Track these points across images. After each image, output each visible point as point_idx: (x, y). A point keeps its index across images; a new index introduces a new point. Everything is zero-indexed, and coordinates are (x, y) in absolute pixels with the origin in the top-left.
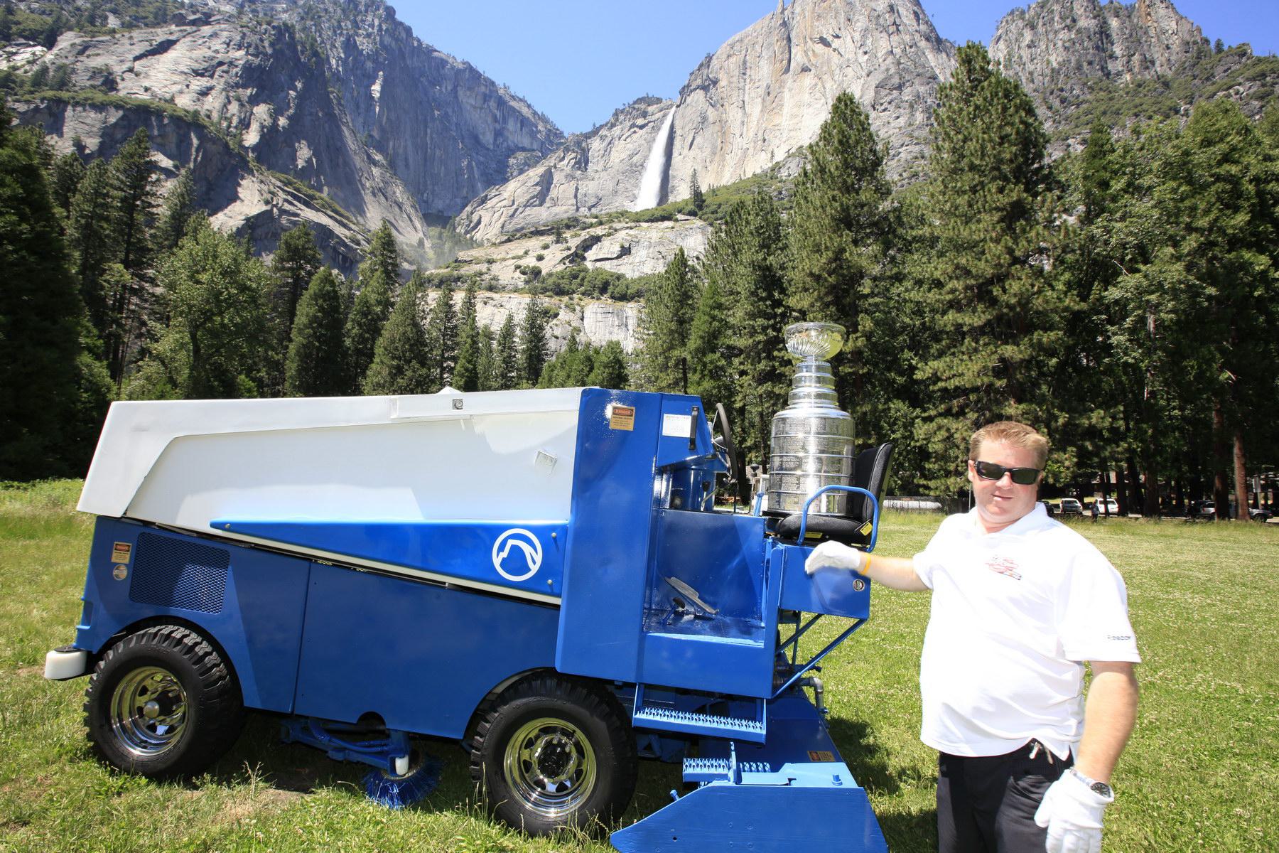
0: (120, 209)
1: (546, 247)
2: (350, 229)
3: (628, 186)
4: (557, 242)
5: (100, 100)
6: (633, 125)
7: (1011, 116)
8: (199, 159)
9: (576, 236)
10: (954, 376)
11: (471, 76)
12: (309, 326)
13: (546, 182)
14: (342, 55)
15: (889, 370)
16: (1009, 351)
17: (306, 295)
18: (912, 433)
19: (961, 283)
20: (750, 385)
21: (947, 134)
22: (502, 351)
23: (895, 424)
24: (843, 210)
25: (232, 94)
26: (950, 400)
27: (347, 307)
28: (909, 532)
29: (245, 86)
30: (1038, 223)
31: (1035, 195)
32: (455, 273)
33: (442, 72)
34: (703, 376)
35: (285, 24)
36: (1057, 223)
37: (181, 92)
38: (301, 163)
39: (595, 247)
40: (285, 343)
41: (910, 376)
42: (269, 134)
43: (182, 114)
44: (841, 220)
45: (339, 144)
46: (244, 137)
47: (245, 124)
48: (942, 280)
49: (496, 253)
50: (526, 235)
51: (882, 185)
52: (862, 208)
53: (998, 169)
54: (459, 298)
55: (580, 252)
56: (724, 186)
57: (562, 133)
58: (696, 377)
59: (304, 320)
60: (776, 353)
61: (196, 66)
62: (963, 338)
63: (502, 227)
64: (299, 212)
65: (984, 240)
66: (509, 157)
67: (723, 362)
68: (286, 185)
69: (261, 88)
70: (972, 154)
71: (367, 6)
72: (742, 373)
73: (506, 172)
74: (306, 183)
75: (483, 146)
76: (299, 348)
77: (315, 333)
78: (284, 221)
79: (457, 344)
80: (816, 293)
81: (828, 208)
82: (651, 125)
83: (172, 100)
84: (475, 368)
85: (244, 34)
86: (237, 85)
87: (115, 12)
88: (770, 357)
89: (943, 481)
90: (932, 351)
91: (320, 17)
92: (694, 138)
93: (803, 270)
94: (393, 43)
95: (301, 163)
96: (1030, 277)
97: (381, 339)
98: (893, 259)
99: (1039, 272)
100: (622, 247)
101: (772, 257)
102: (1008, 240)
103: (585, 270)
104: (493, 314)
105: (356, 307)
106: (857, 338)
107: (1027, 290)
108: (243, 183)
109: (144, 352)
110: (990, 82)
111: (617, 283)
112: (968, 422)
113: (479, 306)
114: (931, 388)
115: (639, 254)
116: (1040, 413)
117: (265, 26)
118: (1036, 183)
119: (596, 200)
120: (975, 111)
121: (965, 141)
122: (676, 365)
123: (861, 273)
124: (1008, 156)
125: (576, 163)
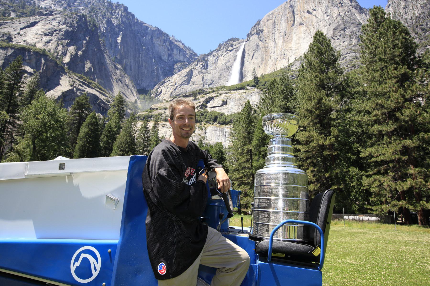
0: (8, 89)
2: (106, 96)
4: (195, 100)
5: (5, 45)
6: (227, 50)
7: (398, 36)
8: (44, 68)
9: (203, 97)
10: (380, 155)
11: (159, 33)
12: (85, 137)
13: (190, 74)
14: (106, 26)
15: (348, 153)
16: (407, 142)
17: (84, 124)
18: (361, 183)
19: (380, 111)
21: (366, 45)
23: (352, 178)
24: (321, 81)
25: (59, 42)
26: (379, 167)
27: (102, 129)
28: (364, 233)
29: (65, 39)
30: (416, 82)
31: (413, 70)
32: (150, 114)
33: (146, 31)
34: (260, 157)
35: (83, 15)
36: (426, 82)
37: (39, 42)
38: (86, 69)
39: (211, 102)
40: (74, 145)
42: (74, 58)
43: (38, 50)
44: (319, 85)
45: (103, 61)
46: (64, 59)
47: (64, 54)
48: (370, 110)
51: (338, 70)
52: (330, 80)
53: (393, 59)
54: (151, 125)
56: (268, 74)
61: (46, 32)
62: (383, 137)
63: (171, 94)
64: (85, 89)
65: (389, 91)
66: (174, 65)
68: (80, 78)
69: (72, 40)
70: (380, 54)
71: (116, 7)
73: (173, 71)
74: (89, 77)
75: (163, 61)
77: (87, 140)
78: (78, 93)
79: (150, 144)
80: (310, 118)
81: (314, 81)
82: (235, 50)
83: (35, 45)
85: (66, 19)
86: (62, 39)
87: (14, 11)
89: (379, 206)
90: (368, 144)
91: (97, 11)
92: (254, 54)
93: (304, 108)
94: (127, 21)
95: (86, 69)
96: (415, 108)
97: (116, 143)
98: (346, 102)
99: (419, 105)
101: (289, 103)
102: (401, 91)
103: (207, 112)
104: (166, 132)
105: (106, 129)
107: (414, 113)
108: (62, 78)
109: (12, 149)
110: (386, 22)
111: (221, 117)
112: (390, 177)
113: (160, 128)
114: (369, 161)
115: (231, 104)
116: (428, 173)
117: (74, 16)
118: (413, 65)
120: (380, 35)
121: (376, 49)
122: (247, 153)
123: (331, 109)
124: (398, 53)
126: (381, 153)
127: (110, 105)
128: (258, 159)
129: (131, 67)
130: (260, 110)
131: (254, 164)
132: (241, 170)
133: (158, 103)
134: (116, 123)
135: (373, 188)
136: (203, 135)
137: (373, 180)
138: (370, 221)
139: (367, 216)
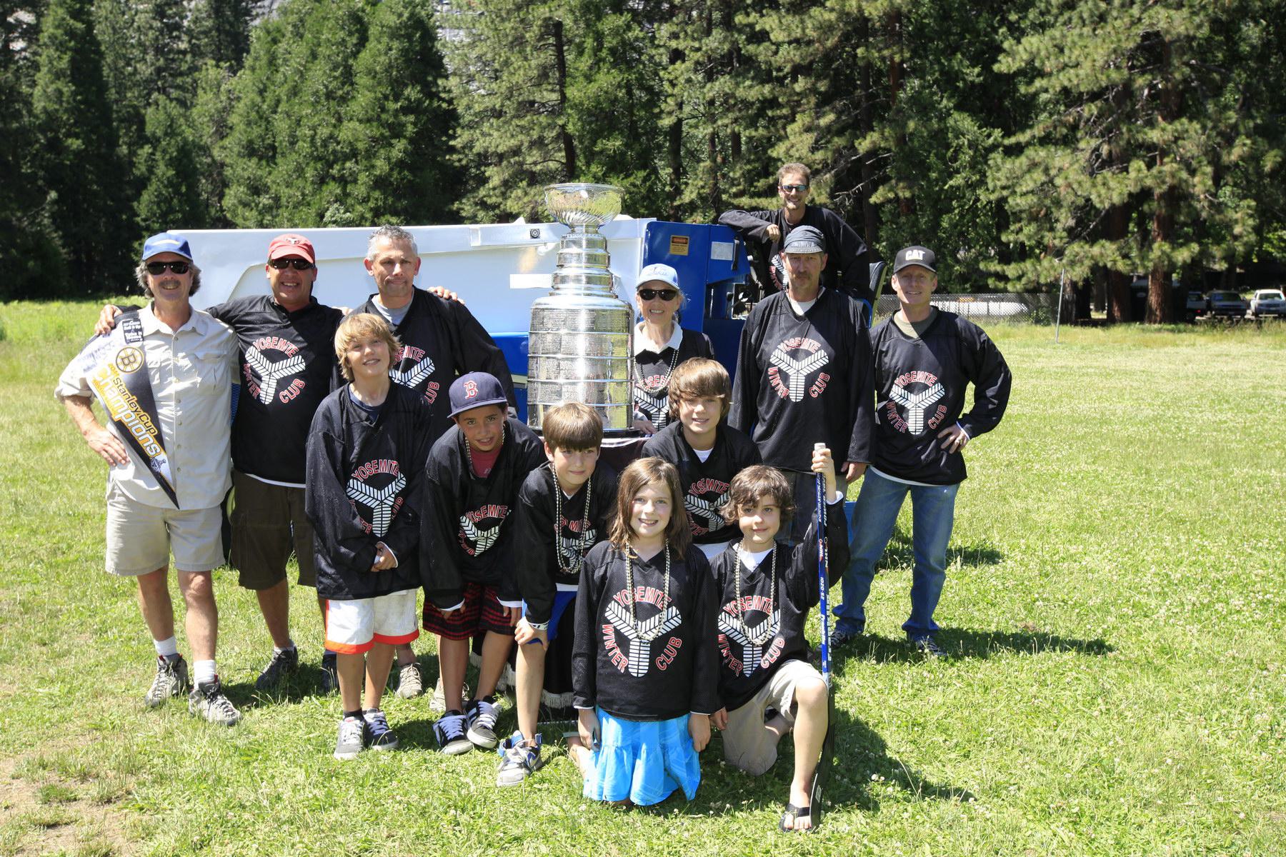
10: (1065, 66)
15: (952, 50)
18: (984, 175)
20: (689, 81)
23: (954, 159)
34: (598, 62)
41: (987, 69)
58: (585, 63)
60: (739, 19)
67: (636, 32)
72: (677, 56)
84: (90, 26)
88: (728, 24)
89: (1028, 265)
112: (1083, 157)
122: (541, 38)
126: (1066, 59)
128: (591, 68)
131: (573, 92)
132: (513, 117)
135: (1024, 194)
137: (1025, 168)
138: (993, 317)
139: (987, 300)
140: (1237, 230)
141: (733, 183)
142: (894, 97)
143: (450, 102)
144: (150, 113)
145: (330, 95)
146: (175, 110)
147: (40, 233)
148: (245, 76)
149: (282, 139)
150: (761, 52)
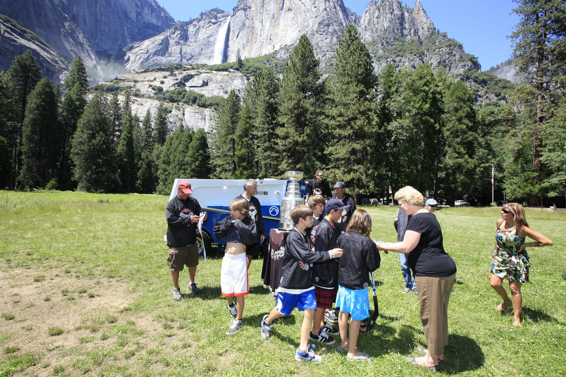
1: (165, 77)
3: (206, 51)
4: (171, 75)
9: (181, 73)
12: (37, 109)
15: (315, 149)
17: (34, 93)
20: (261, 152)
22: (146, 129)
34: (242, 147)
39: (190, 80)
49: (139, 77)
50: (154, 70)
55: (183, 82)
57: (173, 19)
58: (239, 147)
59: (33, 105)
60: (272, 140)
63: (142, 63)
67: (250, 141)
68: (5, 22)
72: (258, 147)
75: (130, 19)
76: (31, 120)
79: (122, 124)
84: (132, 135)
88: (269, 141)
100: (204, 82)
101: (272, 99)
103: (185, 91)
104: (138, 109)
106: (304, 136)
112: (341, 171)
115: (211, 85)
119: (191, 56)
121: (346, 63)
122: (230, 141)
125: (181, 36)
127: (59, 67)
129: (84, 19)
130: (245, 101)
133: (125, 73)
134: (77, 95)
135: (330, 178)
136: (180, 116)
140: (371, 187)
141: (270, 173)
142: (304, 157)
143: (209, 154)
144: (143, 154)
145: (183, 151)
146: (148, 153)
147: (116, 179)
148: (165, 147)
149: (172, 160)
150: (276, 147)
